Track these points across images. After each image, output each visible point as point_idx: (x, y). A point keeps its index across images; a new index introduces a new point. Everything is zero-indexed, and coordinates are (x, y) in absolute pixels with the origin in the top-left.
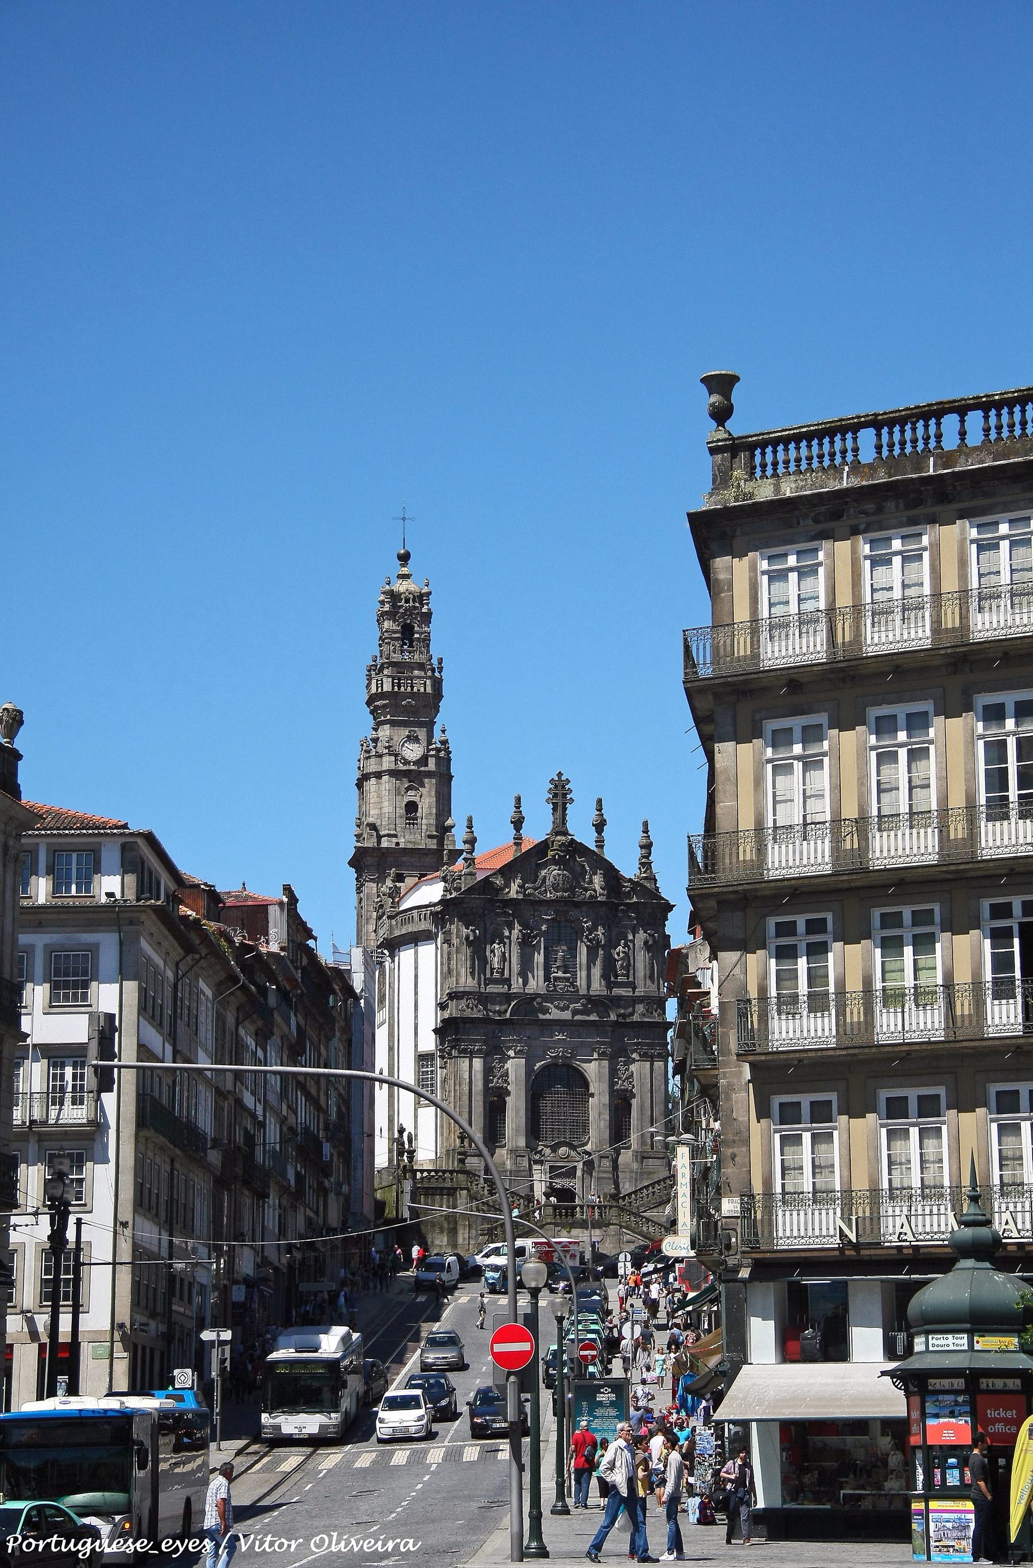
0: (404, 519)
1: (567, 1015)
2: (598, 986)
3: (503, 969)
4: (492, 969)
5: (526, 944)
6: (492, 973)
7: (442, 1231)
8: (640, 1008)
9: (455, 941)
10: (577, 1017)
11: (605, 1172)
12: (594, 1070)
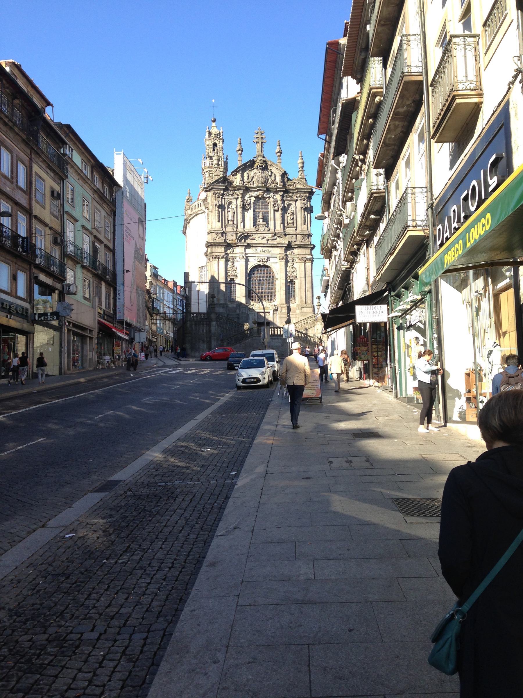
0: (213, 107)
1: (264, 241)
2: (279, 228)
3: (233, 221)
4: (228, 220)
5: (244, 208)
6: (228, 223)
7: (203, 342)
8: (299, 237)
9: (210, 207)
10: (270, 242)
11: (283, 314)
12: (277, 267)
